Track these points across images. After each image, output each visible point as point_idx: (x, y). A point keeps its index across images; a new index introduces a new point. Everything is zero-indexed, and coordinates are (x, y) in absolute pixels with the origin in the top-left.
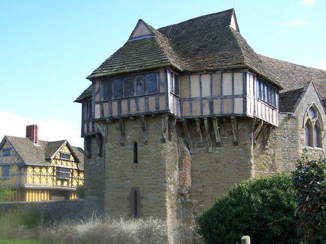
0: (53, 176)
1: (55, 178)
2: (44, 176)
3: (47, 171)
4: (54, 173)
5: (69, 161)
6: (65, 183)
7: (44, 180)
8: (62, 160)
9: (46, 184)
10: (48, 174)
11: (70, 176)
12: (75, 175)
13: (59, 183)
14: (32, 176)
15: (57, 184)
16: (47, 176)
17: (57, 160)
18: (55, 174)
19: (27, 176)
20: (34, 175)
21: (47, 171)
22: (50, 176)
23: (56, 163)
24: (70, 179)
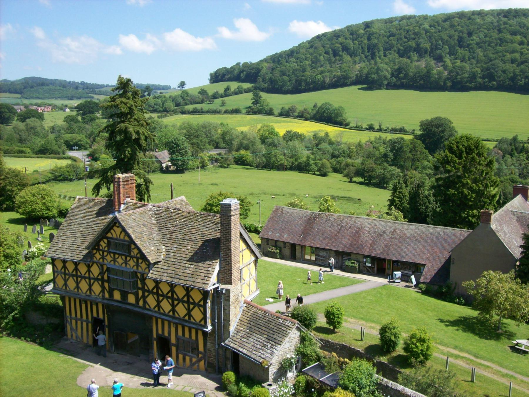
0: (103, 280)
1: (106, 285)
2: (85, 278)
3: (89, 271)
4: (103, 277)
5: (132, 257)
6: (131, 299)
7: (84, 286)
8: (115, 254)
9: (88, 293)
10: (92, 276)
11: (140, 286)
12: (151, 285)
13: (117, 295)
14: (63, 276)
15: (111, 295)
16: (89, 278)
17: (105, 254)
18: (106, 277)
19: (56, 274)
20: (65, 274)
21: (89, 271)
22: (96, 279)
23: (103, 258)
24: (140, 293)
